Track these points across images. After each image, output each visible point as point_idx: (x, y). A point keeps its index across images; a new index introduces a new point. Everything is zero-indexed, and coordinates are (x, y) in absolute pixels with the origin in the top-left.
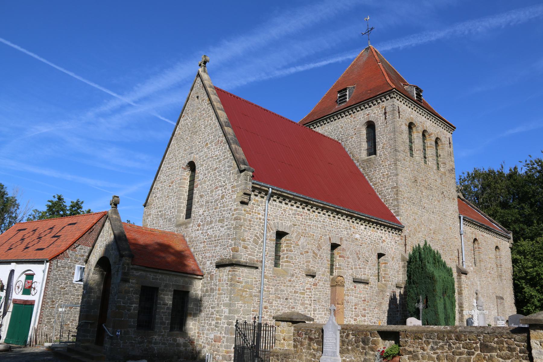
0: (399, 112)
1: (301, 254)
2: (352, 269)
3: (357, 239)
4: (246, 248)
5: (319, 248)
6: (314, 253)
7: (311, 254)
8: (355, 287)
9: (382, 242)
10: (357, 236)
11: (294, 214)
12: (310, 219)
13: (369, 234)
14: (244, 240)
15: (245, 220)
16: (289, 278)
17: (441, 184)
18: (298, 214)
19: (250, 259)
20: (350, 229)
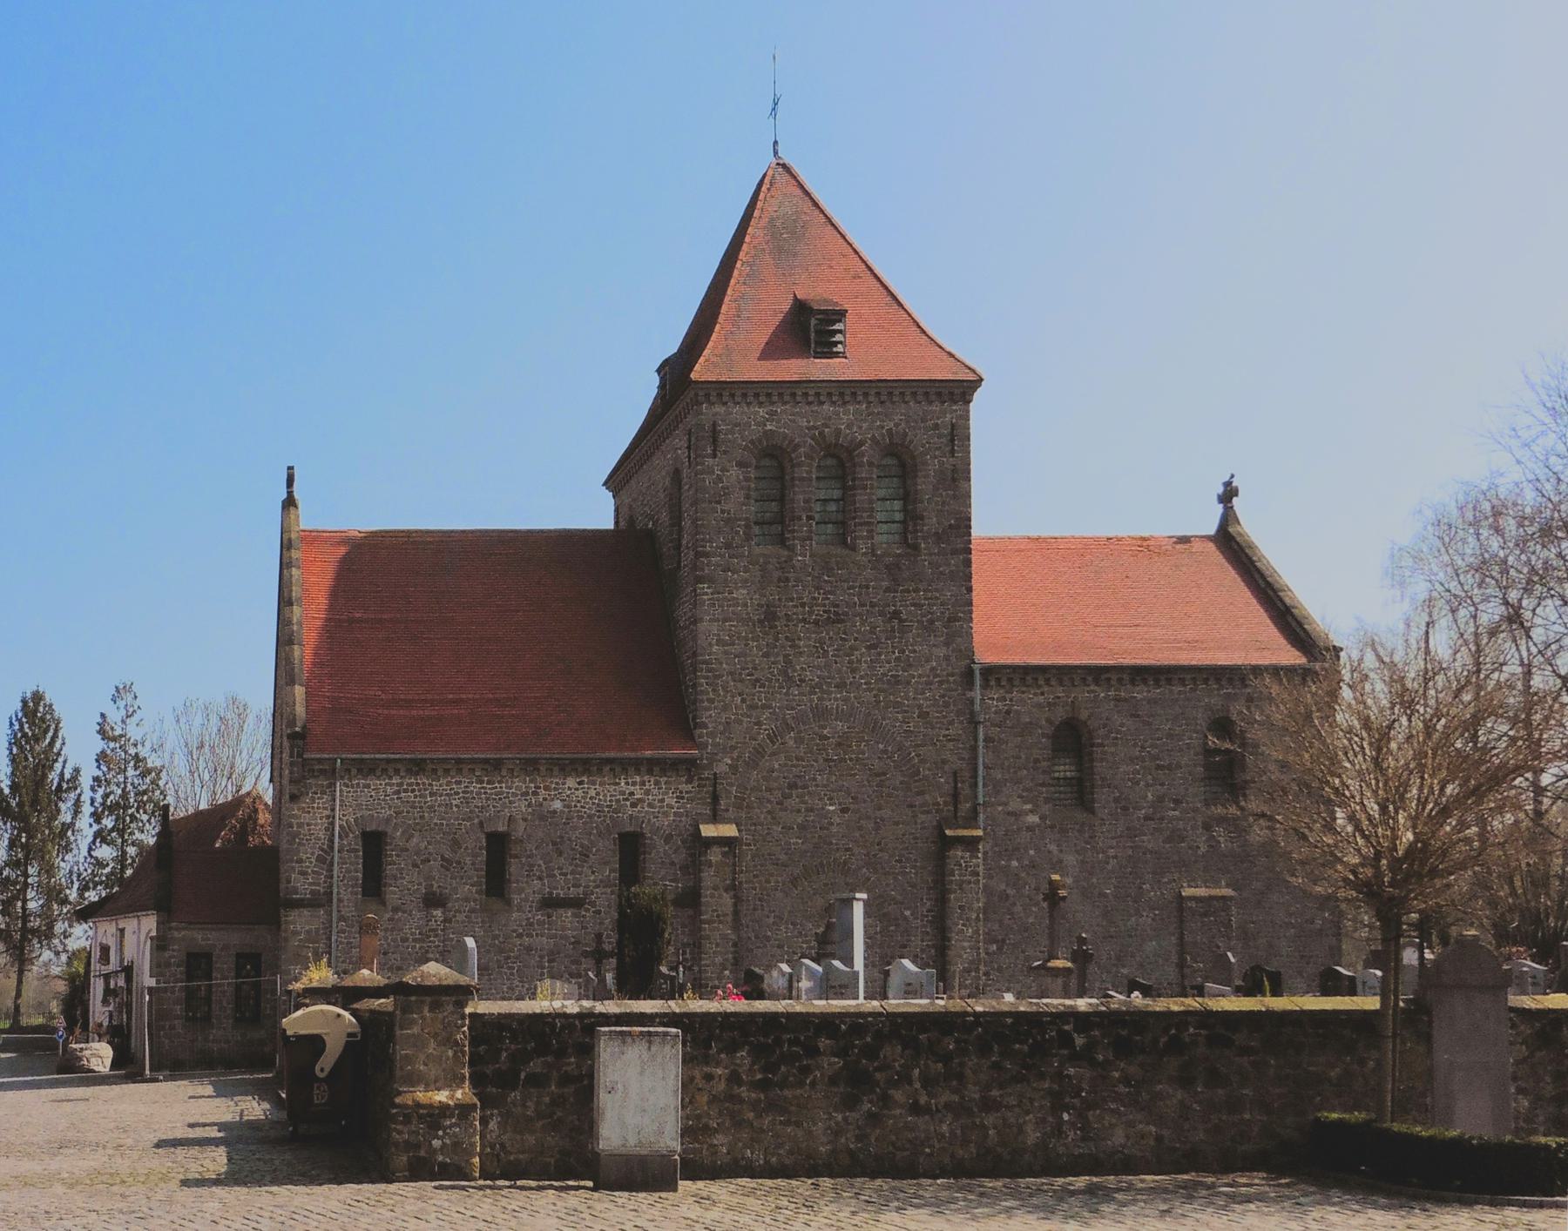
0: (715, 441)
1: (415, 865)
2: (540, 878)
3: (555, 812)
4: (303, 873)
5: (456, 844)
6: (443, 858)
7: (435, 864)
8: (549, 916)
9: (634, 805)
10: (557, 805)
11: (398, 792)
12: (432, 794)
13: (592, 793)
14: (300, 861)
15: (300, 825)
16: (387, 916)
17: (887, 590)
18: (406, 791)
19: (312, 892)
20: (535, 793)
